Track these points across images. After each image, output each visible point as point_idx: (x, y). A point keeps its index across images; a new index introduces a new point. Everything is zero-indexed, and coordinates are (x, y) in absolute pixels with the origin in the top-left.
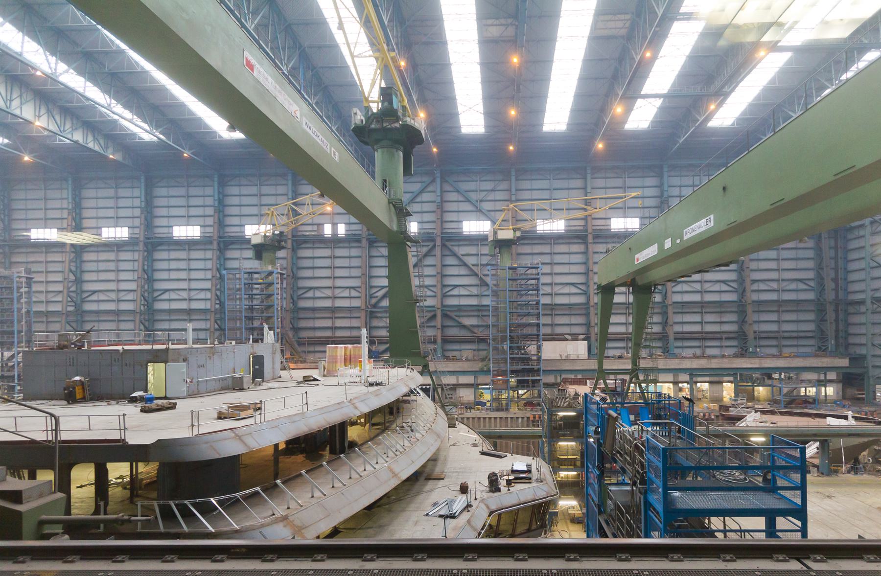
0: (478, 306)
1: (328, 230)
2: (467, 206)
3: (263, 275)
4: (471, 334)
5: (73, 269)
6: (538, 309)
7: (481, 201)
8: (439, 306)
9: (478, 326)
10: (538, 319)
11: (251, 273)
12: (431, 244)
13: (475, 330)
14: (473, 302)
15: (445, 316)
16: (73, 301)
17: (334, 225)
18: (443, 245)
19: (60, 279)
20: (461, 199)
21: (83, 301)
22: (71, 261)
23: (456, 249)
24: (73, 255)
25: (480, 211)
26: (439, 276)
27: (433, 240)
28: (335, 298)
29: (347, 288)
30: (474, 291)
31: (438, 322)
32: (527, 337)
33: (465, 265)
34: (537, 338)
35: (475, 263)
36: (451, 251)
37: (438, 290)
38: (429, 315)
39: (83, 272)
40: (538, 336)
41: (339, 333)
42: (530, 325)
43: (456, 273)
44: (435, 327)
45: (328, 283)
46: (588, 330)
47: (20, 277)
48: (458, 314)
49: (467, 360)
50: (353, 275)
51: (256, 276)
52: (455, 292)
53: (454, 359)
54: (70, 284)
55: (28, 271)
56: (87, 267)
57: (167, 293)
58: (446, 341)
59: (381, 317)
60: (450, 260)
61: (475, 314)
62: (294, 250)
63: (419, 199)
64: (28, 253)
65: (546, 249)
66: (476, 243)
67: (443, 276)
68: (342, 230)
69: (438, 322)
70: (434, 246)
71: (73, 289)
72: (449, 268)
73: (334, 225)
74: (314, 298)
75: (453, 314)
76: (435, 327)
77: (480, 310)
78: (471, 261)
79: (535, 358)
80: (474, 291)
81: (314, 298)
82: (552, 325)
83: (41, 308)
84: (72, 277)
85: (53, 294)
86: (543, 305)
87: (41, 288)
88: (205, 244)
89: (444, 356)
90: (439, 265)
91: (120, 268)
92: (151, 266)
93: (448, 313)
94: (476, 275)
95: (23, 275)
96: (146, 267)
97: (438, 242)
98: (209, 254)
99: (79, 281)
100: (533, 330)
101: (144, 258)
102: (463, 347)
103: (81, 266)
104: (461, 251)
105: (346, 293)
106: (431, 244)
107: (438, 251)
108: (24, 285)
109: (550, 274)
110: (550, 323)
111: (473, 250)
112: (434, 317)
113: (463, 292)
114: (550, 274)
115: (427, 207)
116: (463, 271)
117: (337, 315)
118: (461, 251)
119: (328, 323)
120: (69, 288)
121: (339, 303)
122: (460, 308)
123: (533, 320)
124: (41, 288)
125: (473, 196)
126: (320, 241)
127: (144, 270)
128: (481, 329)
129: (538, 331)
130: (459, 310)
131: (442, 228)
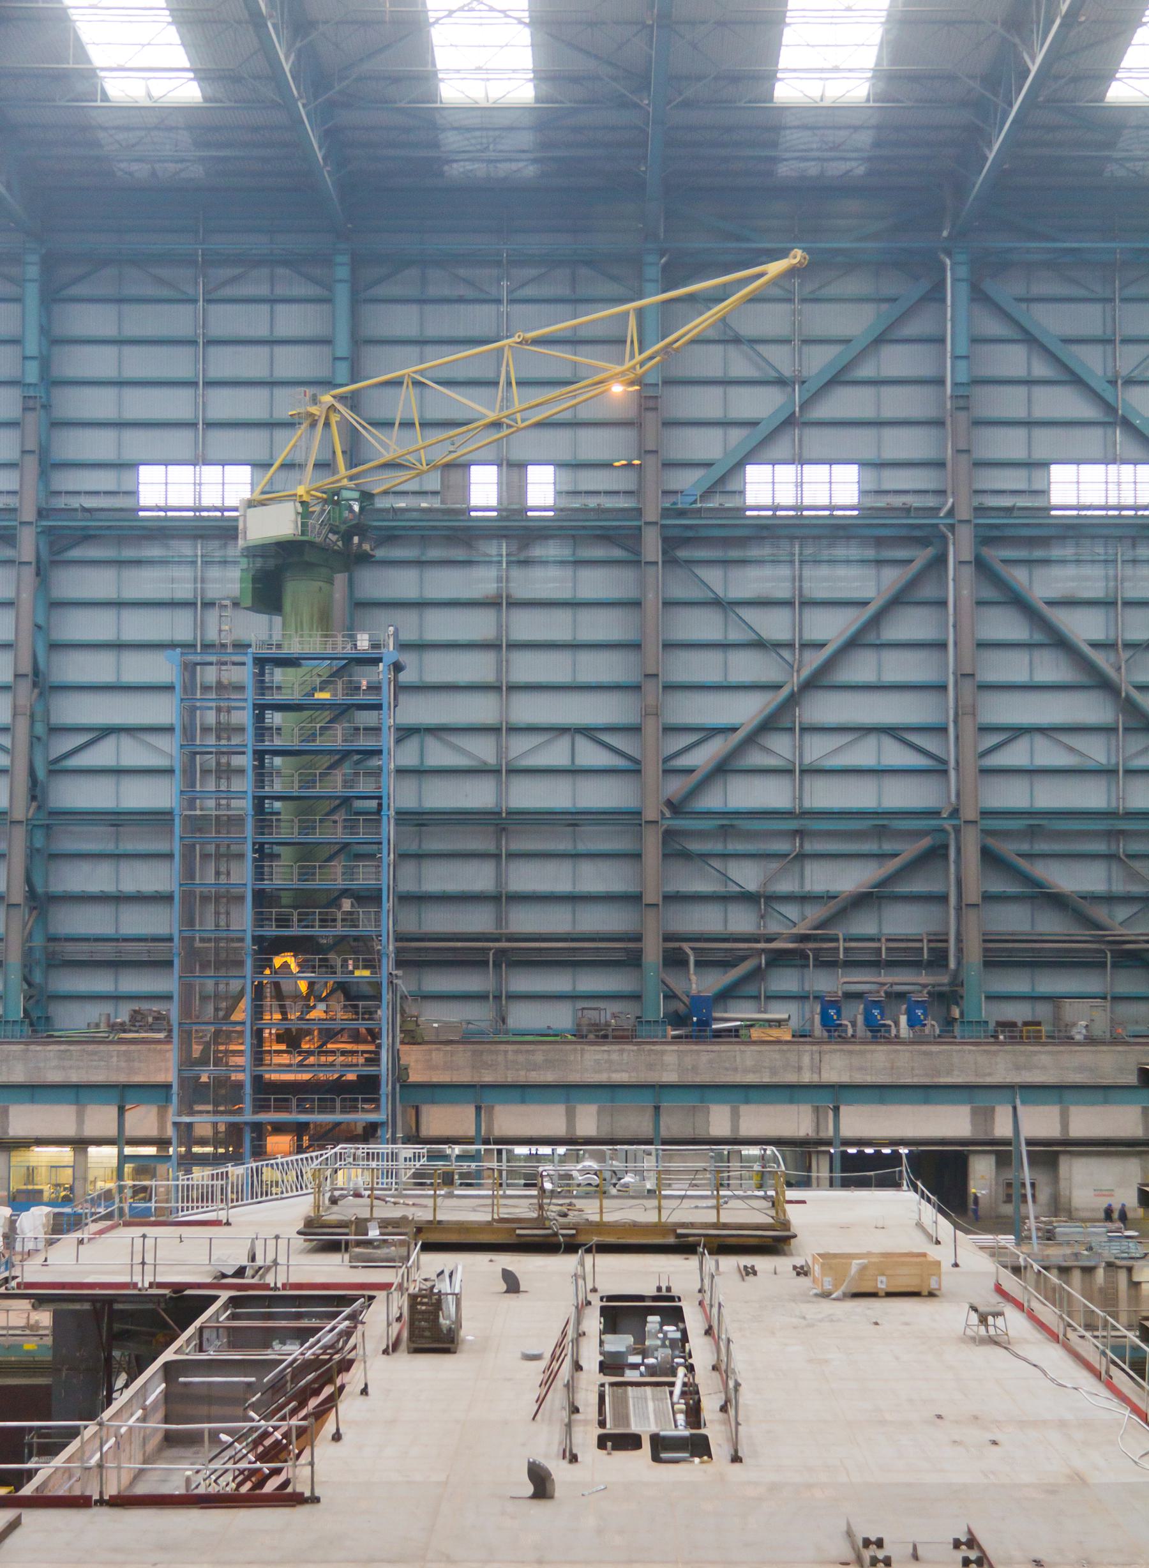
1: (484, 488)
2: (1065, 403)
7: (1130, 382)
9: (1110, 899)
13: (1100, 913)
14: (1091, 796)
17: (513, 469)
20: (1041, 370)
23: (1019, 576)
25: (1127, 424)
29: (562, 730)
30: (1096, 751)
33: (1061, 643)
35: (1099, 635)
38: (910, 850)
41: (526, 921)
43: (1022, 677)
45: (480, 709)
48: (1025, 847)
50: (584, 677)
52: (1016, 755)
59: (704, 857)
61: (1100, 847)
63: (866, 371)
68: (542, 488)
73: (513, 469)
78: (1084, 627)
80: (1096, 751)
105: (557, 754)
113: (1048, 754)
115: (898, 403)
116: (1050, 668)
117: (516, 846)
119: (478, 878)
121: (528, 795)
122: (1037, 824)
125: (1092, 361)
126: (458, 534)
128: (1122, 913)
130: (1032, 833)
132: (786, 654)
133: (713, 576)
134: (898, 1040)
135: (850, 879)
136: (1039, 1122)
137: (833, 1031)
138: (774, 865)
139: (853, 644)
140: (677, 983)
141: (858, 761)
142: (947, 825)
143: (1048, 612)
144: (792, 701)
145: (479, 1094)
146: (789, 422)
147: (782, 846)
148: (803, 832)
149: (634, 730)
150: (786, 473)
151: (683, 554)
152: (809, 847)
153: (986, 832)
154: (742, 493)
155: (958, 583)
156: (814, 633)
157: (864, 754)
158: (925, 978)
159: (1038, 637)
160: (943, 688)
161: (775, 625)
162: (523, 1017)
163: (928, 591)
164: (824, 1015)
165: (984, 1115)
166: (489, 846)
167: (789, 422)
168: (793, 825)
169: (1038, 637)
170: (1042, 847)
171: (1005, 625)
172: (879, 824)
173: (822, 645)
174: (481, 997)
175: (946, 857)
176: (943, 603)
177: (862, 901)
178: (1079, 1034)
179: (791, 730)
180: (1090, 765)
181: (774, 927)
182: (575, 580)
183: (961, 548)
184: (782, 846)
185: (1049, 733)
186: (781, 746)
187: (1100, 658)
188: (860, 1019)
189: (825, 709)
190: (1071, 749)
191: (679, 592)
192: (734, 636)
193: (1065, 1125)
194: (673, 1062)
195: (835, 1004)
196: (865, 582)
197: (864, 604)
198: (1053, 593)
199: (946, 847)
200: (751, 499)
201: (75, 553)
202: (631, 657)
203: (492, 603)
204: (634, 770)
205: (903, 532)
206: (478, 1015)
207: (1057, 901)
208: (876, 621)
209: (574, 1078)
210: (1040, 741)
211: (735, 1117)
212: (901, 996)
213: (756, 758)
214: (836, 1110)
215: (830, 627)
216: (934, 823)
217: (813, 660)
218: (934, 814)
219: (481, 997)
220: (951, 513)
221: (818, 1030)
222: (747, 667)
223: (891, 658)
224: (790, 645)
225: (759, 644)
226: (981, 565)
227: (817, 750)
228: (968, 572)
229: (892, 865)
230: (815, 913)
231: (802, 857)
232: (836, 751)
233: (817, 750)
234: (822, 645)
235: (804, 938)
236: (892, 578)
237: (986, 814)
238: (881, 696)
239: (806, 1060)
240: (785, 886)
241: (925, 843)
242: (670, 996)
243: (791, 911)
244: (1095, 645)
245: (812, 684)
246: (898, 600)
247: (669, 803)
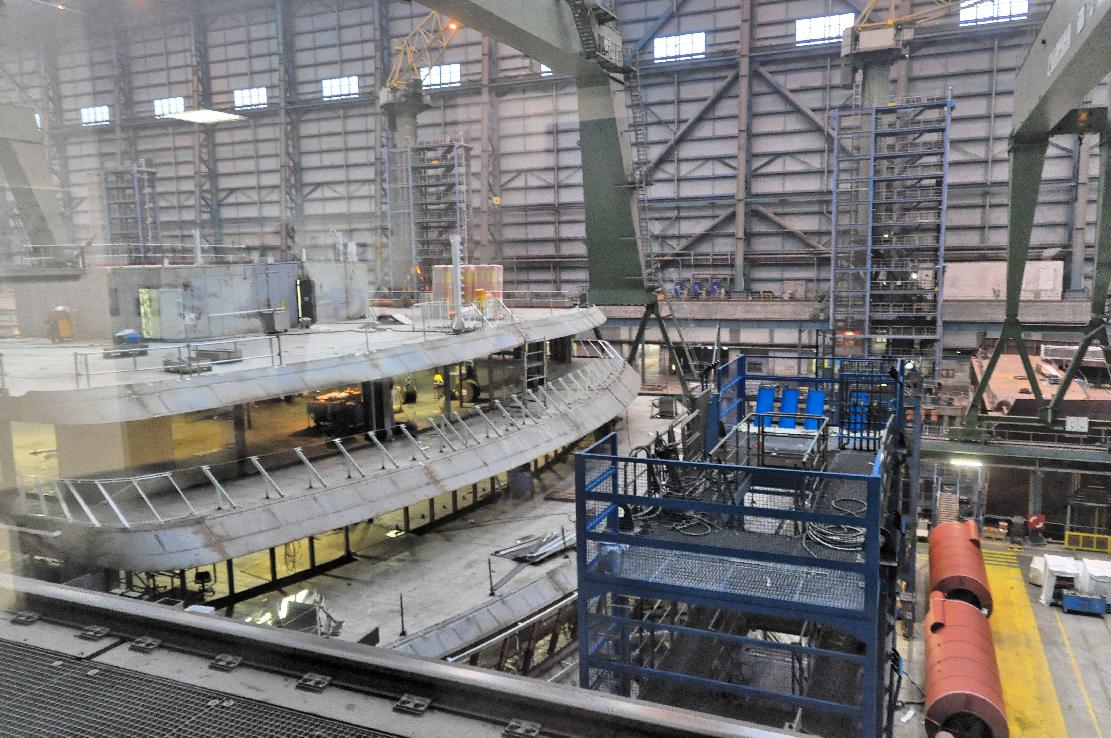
0: (821, 193)
3: (439, 153)
4: (803, 250)
5: (205, 157)
6: (940, 193)
8: (742, 195)
10: (939, 215)
11: (423, 149)
12: (731, 74)
13: (813, 241)
14: (812, 184)
15: (753, 214)
16: (208, 205)
18: (755, 75)
19: (192, 173)
21: (220, 205)
22: (201, 145)
23: (779, 80)
24: (203, 136)
26: (744, 136)
27: (735, 66)
28: (560, 187)
30: (815, 162)
31: (738, 228)
32: (913, 253)
33: (797, 110)
34: (933, 254)
35: (818, 105)
36: (769, 84)
37: (740, 164)
38: (723, 214)
39: (216, 161)
40: (936, 250)
42: (919, 229)
44: (732, 235)
46: (1070, 238)
47: (141, 172)
48: (779, 210)
49: (792, 298)
51: (430, 154)
52: (777, 167)
53: (769, 297)
54: (203, 180)
55: (149, 163)
56: (222, 152)
57: (320, 189)
58: (752, 262)
60: (768, 103)
64: (156, 136)
65: (981, 61)
66: (821, 63)
67: (751, 136)
69: (738, 228)
70: (736, 78)
71: (207, 187)
72: (764, 120)
75: (769, 212)
76: (732, 235)
77: (821, 201)
78: (806, 102)
79: (930, 297)
80: (815, 162)
82: (982, 228)
83: (173, 216)
84: (204, 169)
85: (268, 190)
86: (951, 186)
87: (171, 187)
88: (366, 106)
89: (748, 290)
90: (744, 116)
91: (261, 153)
92: (297, 147)
93: (761, 208)
94: (819, 130)
95: (144, 169)
96: (291, 150)
97: (744, 69)
98: (371, 123)
99: (213, 176)
100: (928, 240)
101: (286, 134)
102: (788, 274)
103: (214, 153)
106: (731, 74)
107: (743, 87)
108: (146, 184)
109: (987, 117)
110: (978, 223)
111: (814, 78)
112: (732, 217)
113: (792, 165)
114: (987, 117)
116: (793, 123)
117: (564, 218)
118: (790, 82)
120: (201, 186)
122: (783, 199)
123: (928, 219)
124: (171, 187)
127: (288, 153)
129: (937, 239)
130: (784, 203)
131: (752, 38)
135: (699, 228)
138: (667, 222)
139: (700, 119)
141: (705, 173)
143: (791, 96)
146: (672, 16)
148: (679, 207)
150: (673, 40)
152: (683, 214)
154: (652, 52)
157: (707, 170)
159: (789, 108)
161: (668, 113)
166: (551, 218)
167: (672, 16)
168: (674, 204)
169: (789, 108)
172: (712, 202)
173: (686, 121)
177: (703, 238)
180: (813, 169)
181: (667, 250)
184: (668, 214)
185: (798, 156)
186: (670, 169)
187: (817, 118)
189: (688, 150)
190: (804, 162)
192: (650, 119)
193: (772, 338)
196: (708, 90)
197: (705, 99)
200: (657, 55)
201: (305, 117)
205: (724, 63)
206: (548, 289)
207: (791, 235)
210: (788, 160)
213: (660, 175)
215: (691, 112)
217: (684, 127)
225: (660, 123)
227: (686, 169)
229: (717, 220)
230: (684, 242)
231: (678, 218)
232: (694, 170)
233: (686, 169)
234: (686, 121)
235: (678, 255)
238: (719, 140)
240: (671, 232)
243: (674, 243)
246: (720, 97)
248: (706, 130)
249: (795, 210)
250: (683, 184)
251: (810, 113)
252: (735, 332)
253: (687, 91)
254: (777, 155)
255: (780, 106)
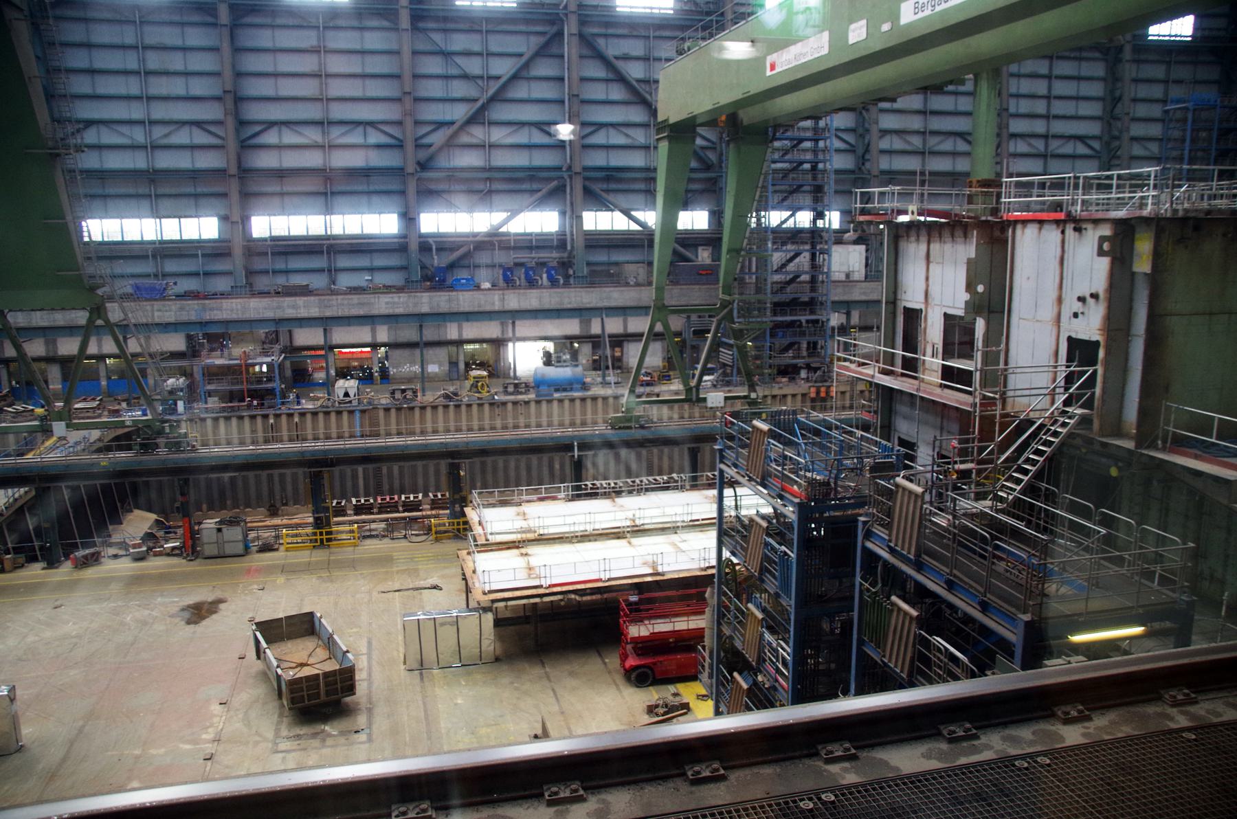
33: (621, 79)
43: (602, 97)
62: (234, 28)
74: (280, 147)
81: (280, 147)
104: (613, 49)
106: (554, 29)
116: (617, 93)
130: (608, 179)
132: (480, 82)
133: (437, 37)
134: (542, 287)
136: (614, 326)
137: (509, 283)
139: (515, 77)
140: (427, 261)
142: (565, 175)
144: (483, 108)
145: (326, 323)
147: (481, 186)
149: (399, 123)
151: (421, 25)
153: (586, 179)
155: (570, 47)
156: (494, 72)
158: (555, 254)
159: (611, 76)
160: (562, 102)
161: (474, 66)
162: (345, 281)
163: (554, 50)
164: (505, 275)
165: (586, 323)
168: (486, 175)
169: (611, 76)
170: (613, 186)
171: (595, 70)
173: (498, 78)
174: (321, 270)
175: (565, 191)
176: (563, 56)
178: (632, 281)
179: (484, 123)
180: (637, 144)
182: (362, 38)
183: (571, 27)
188: (523, 277)
190: (627, 135)
191: (421, 47)
193: (625, 327)
194: (426, 302)
195: (509, 269)
197: (520, 55)
198: (617, 53)
199: (565, 186)
202: (395, 82)
203: (315, 51)
204: (399, 145)
208: (526, 66)
209: (375, 312)
210: (612, 131)
211: (460, 328)
212: (543, 264)
213: (465, 139)
214: (514, 323)
215: (503, 68)
216: (559, 174)
217: (494, 87)
218: (559, 169)
219: (321, 270)
220: (566, 7)
221: (501, 283)
222: (460, 89)
223: (534, 85)
224: (482, 77)
225: (465, 76)
226: (581, 36)
228: (575, 40)
233: (497, 135)
236: (536, 42)
237: (585, 169)
239: (496, 297)
241: (555, 183)
242: (423, 267)
244: (638, 81)
245: (495, 99)
247: (419, 163)
248: (520, 91)
249: (620, 186)
250: (493, 152)
251: (635, 83)
252: (586, 323)
253: (496, 44)
254: (601, 126)
255: (601, 73)
